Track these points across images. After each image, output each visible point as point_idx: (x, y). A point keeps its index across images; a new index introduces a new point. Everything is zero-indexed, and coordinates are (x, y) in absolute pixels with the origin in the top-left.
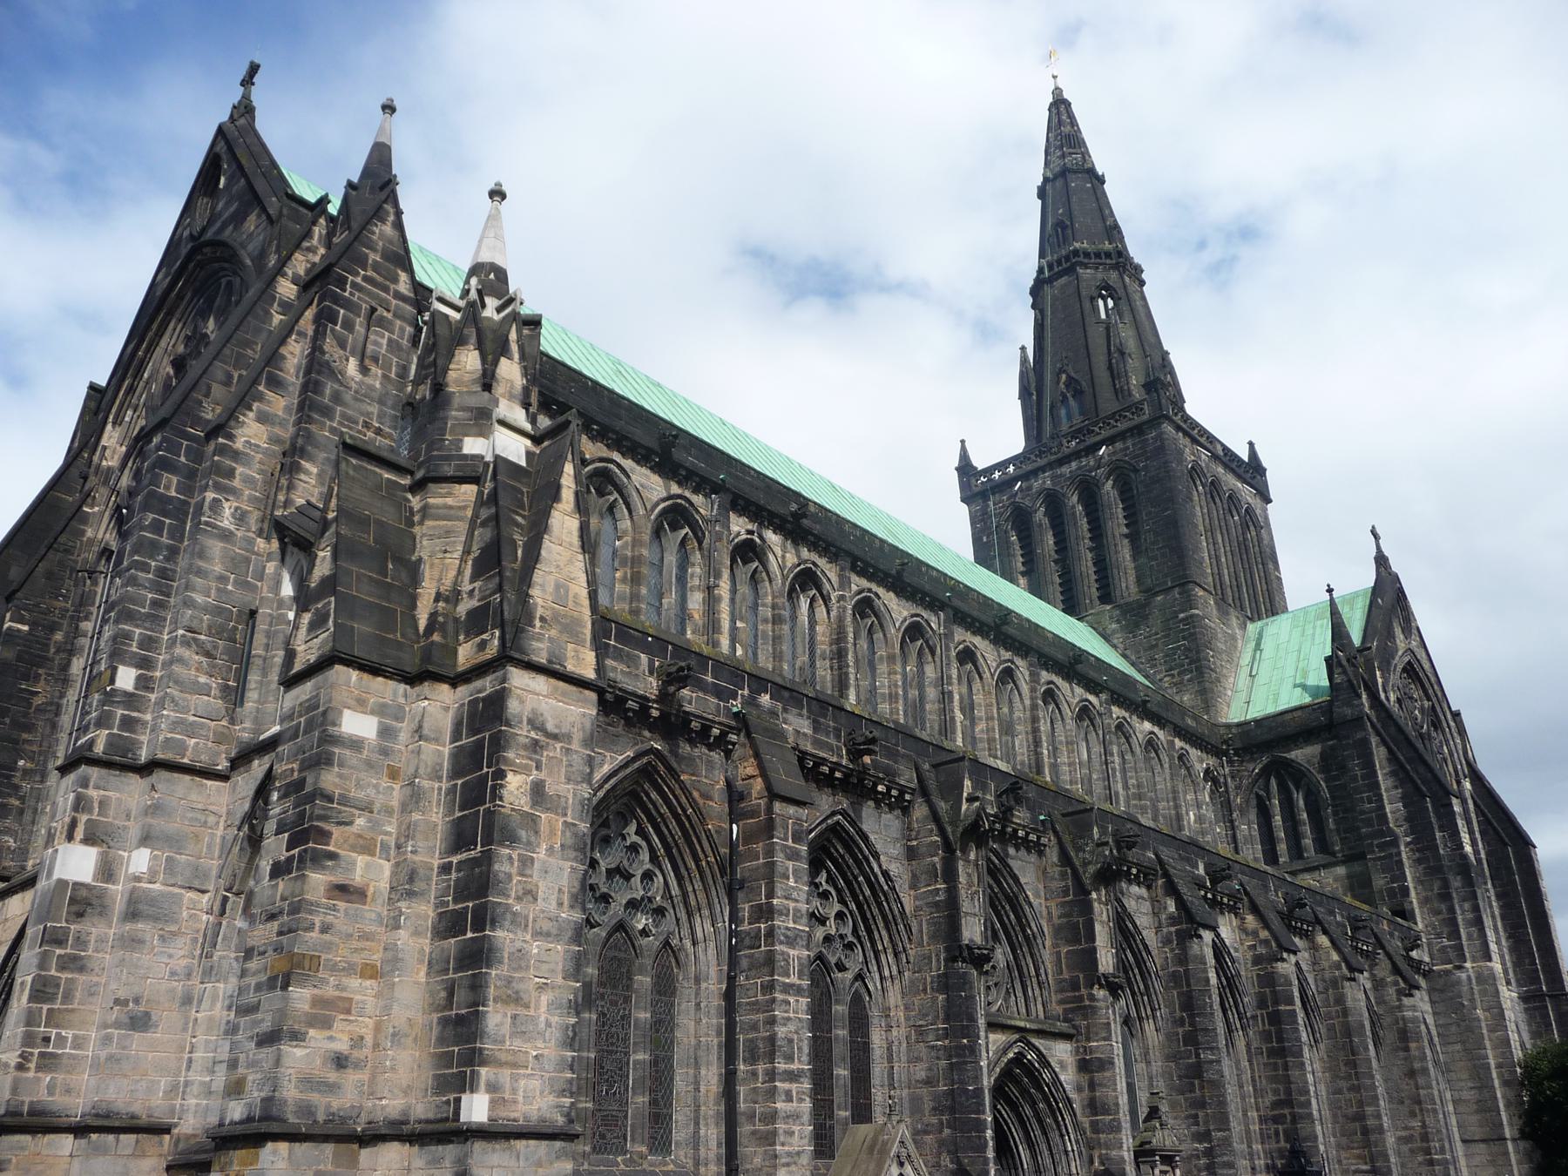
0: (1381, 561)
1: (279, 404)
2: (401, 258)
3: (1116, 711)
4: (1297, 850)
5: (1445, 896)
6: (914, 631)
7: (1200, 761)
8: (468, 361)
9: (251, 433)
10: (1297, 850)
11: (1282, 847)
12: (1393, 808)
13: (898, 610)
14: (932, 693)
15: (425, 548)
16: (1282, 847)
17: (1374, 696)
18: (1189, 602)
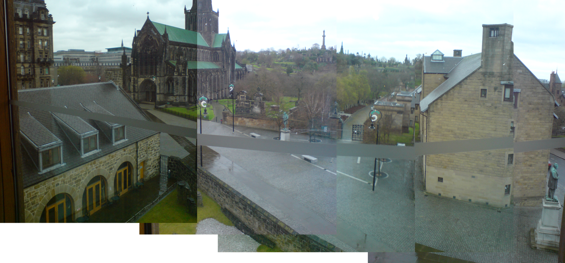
0: (228, 31)
1: (164, 53)
2: (168, 40)
3: (205, 50)
4: (216, 60)
5: (227, 66)
6: (190, 50)
7: (210, 51)
8: (181, 57)
9: (164, 56)
10: (216, 60)
11: (215, 59)
12: (225, 58)
13: (189, 48)
14: (190, 54)
15: (180, 68)
16: (215, 59)
17: (225, 48)
18: (210, 34)
